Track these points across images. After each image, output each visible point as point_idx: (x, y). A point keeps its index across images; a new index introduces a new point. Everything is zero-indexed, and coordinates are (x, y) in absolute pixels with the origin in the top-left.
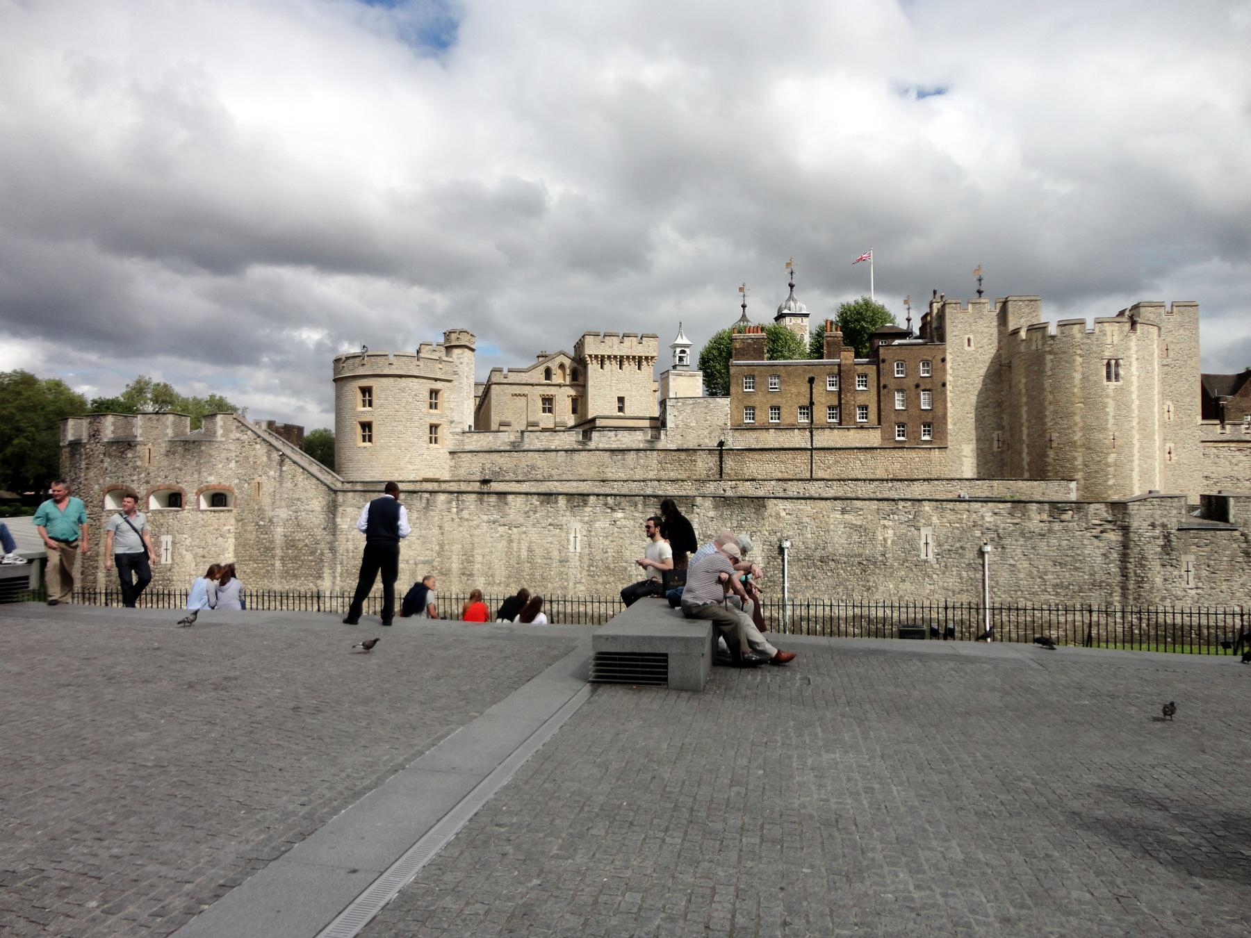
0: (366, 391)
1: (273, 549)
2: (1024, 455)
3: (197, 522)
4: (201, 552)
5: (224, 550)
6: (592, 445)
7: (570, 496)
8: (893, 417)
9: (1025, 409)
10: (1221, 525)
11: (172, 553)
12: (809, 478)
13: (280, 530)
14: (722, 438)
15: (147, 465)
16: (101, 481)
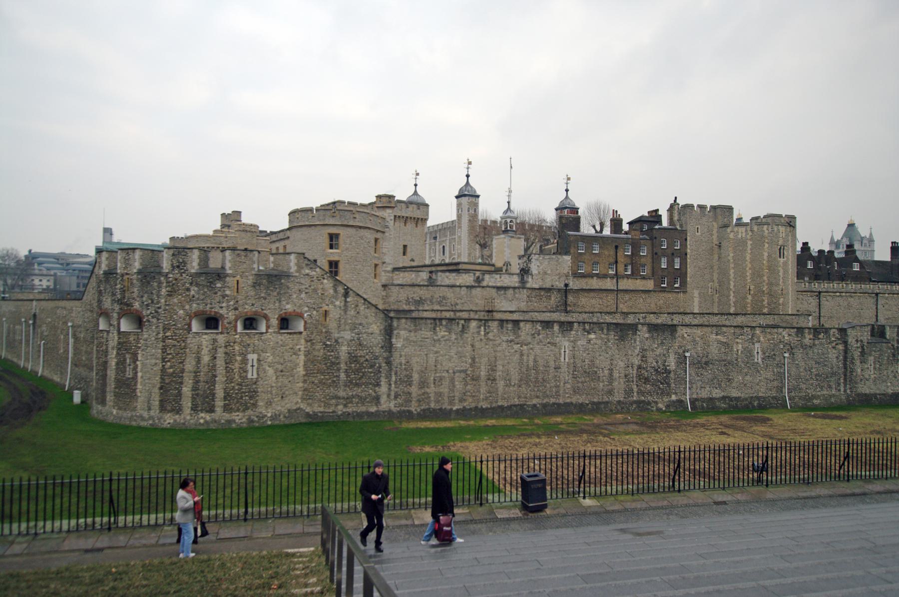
0: (333, 239)
1: (339, 363)
2: (731, 297)
3: (277, 343)
4: (280, 367)
5: (297, 365)
6: (484, 284)
7: (561, 324)
8: (660, 273)
9: (732, 271)
10: (884, 340)
11: (258, 369)
12: (614, 310)
13: (344, 348)
14: (566, 282)
15: (236, 294)
16: (187, 307)
